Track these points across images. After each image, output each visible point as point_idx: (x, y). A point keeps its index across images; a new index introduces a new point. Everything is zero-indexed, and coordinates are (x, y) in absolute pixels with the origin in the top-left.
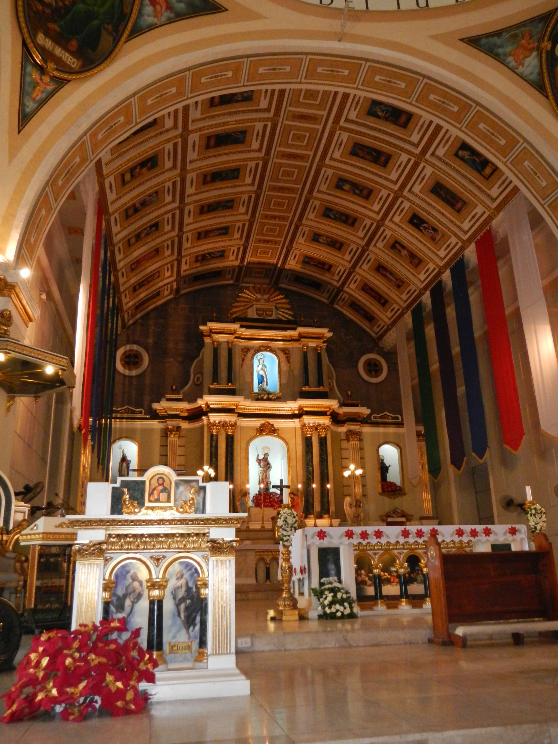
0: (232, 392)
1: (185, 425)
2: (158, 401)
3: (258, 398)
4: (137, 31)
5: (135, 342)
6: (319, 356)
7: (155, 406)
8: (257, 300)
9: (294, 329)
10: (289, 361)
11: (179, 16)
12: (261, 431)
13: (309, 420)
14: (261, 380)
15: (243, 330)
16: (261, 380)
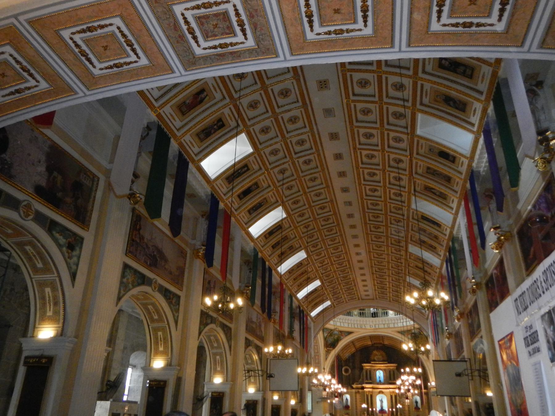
0: (370, 383)
1: (360, 391)
2: (353, 384)
3: (378, 384)
4: (341, 340)
5: (347, 365)
6: (394, 372)
7: (353, 385)
8: (377, 355)
9: (386, 364)
10: (386, 373)
11: (346, 336)
12: (381, 392)
13: (391, 390)
14: (379, 378)
15: (373, 365)
16: (379, 378)
